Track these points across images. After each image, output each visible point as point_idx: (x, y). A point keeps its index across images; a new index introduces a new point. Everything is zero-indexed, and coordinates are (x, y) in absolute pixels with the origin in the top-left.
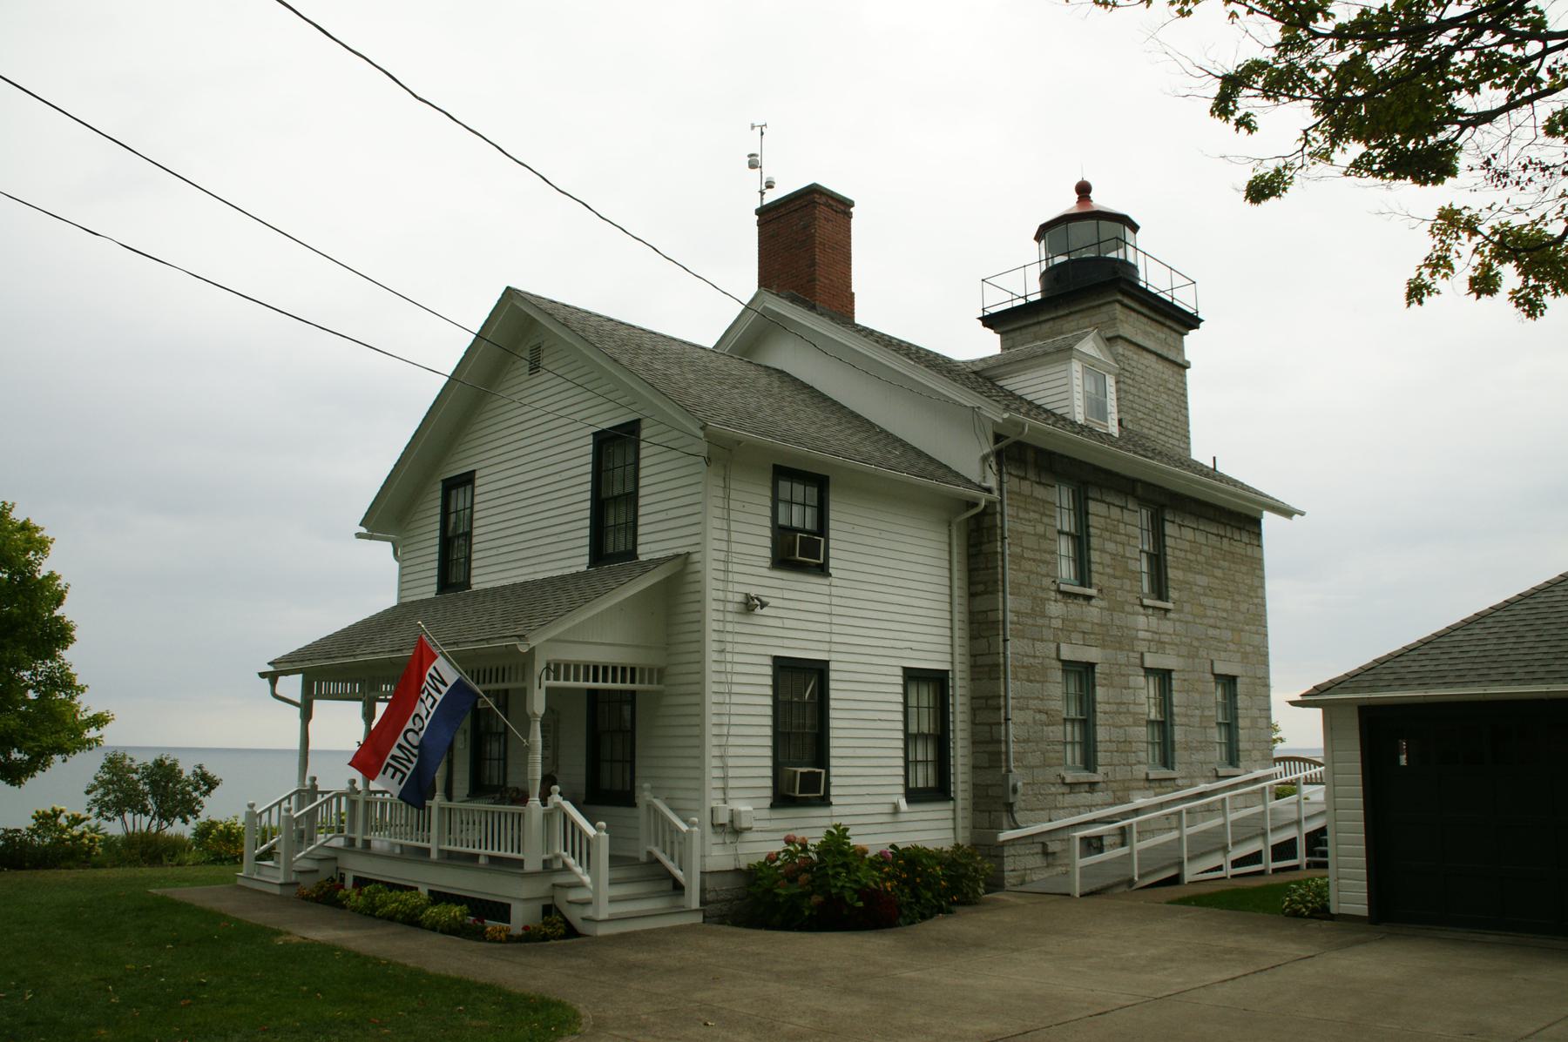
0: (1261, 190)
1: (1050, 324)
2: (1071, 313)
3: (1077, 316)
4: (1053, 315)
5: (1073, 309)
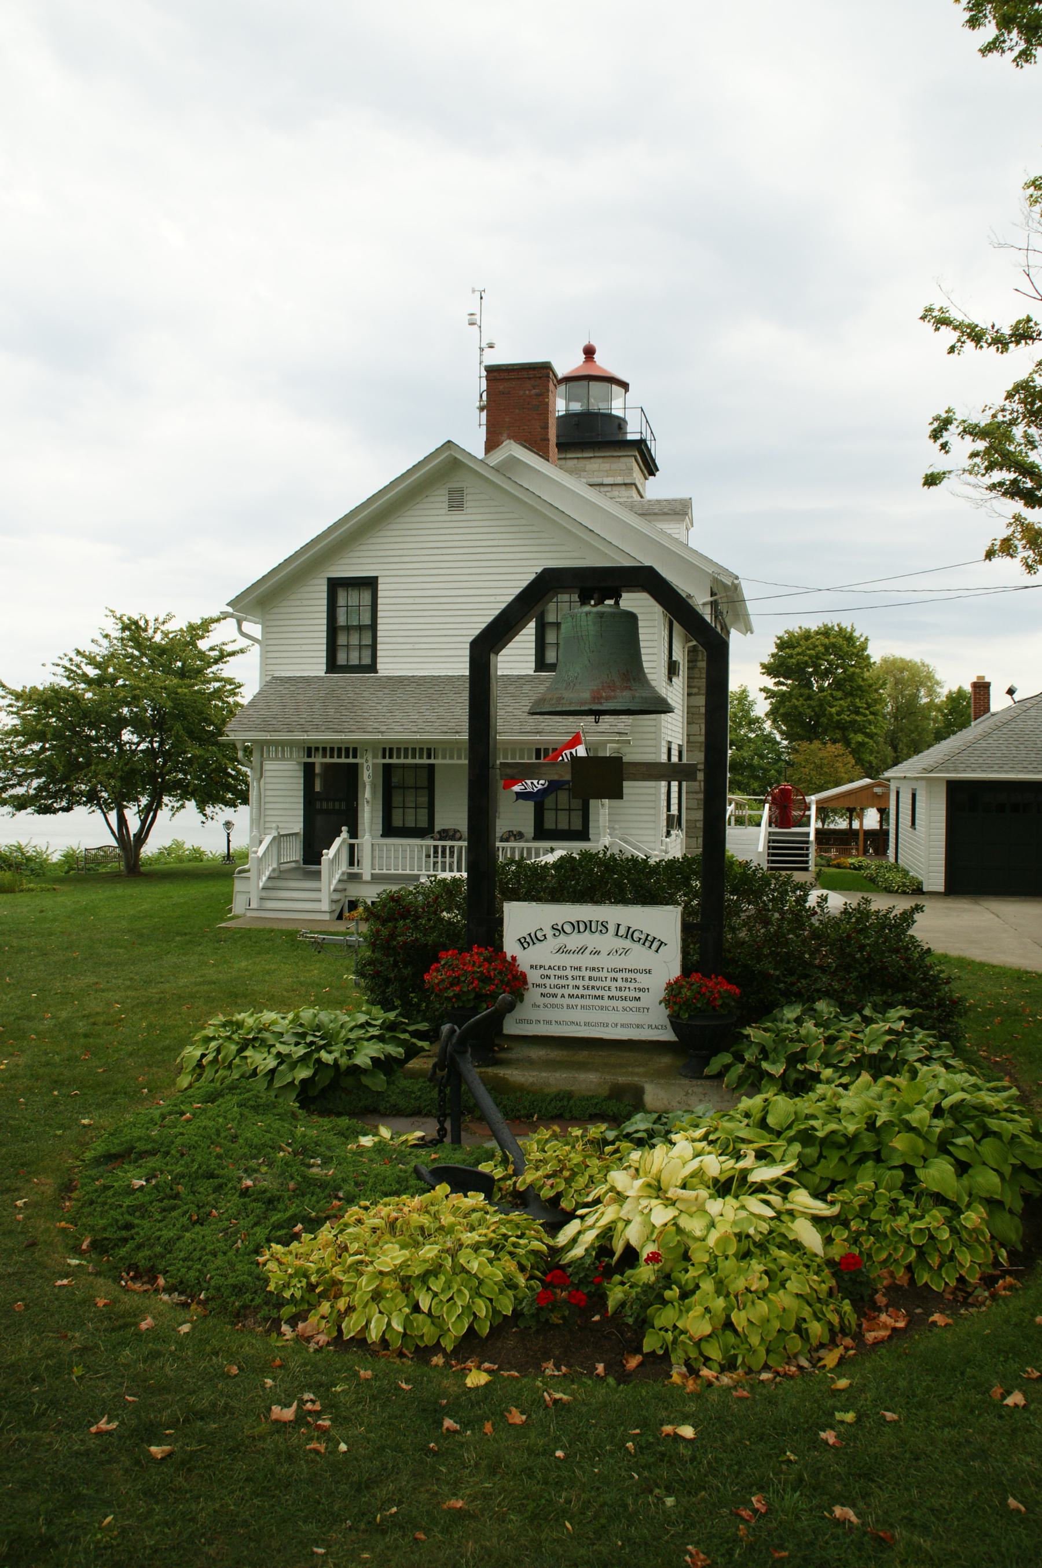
0: (932, 480)
1: (576, 461)
3: (600, 460)
5: (597, 454)
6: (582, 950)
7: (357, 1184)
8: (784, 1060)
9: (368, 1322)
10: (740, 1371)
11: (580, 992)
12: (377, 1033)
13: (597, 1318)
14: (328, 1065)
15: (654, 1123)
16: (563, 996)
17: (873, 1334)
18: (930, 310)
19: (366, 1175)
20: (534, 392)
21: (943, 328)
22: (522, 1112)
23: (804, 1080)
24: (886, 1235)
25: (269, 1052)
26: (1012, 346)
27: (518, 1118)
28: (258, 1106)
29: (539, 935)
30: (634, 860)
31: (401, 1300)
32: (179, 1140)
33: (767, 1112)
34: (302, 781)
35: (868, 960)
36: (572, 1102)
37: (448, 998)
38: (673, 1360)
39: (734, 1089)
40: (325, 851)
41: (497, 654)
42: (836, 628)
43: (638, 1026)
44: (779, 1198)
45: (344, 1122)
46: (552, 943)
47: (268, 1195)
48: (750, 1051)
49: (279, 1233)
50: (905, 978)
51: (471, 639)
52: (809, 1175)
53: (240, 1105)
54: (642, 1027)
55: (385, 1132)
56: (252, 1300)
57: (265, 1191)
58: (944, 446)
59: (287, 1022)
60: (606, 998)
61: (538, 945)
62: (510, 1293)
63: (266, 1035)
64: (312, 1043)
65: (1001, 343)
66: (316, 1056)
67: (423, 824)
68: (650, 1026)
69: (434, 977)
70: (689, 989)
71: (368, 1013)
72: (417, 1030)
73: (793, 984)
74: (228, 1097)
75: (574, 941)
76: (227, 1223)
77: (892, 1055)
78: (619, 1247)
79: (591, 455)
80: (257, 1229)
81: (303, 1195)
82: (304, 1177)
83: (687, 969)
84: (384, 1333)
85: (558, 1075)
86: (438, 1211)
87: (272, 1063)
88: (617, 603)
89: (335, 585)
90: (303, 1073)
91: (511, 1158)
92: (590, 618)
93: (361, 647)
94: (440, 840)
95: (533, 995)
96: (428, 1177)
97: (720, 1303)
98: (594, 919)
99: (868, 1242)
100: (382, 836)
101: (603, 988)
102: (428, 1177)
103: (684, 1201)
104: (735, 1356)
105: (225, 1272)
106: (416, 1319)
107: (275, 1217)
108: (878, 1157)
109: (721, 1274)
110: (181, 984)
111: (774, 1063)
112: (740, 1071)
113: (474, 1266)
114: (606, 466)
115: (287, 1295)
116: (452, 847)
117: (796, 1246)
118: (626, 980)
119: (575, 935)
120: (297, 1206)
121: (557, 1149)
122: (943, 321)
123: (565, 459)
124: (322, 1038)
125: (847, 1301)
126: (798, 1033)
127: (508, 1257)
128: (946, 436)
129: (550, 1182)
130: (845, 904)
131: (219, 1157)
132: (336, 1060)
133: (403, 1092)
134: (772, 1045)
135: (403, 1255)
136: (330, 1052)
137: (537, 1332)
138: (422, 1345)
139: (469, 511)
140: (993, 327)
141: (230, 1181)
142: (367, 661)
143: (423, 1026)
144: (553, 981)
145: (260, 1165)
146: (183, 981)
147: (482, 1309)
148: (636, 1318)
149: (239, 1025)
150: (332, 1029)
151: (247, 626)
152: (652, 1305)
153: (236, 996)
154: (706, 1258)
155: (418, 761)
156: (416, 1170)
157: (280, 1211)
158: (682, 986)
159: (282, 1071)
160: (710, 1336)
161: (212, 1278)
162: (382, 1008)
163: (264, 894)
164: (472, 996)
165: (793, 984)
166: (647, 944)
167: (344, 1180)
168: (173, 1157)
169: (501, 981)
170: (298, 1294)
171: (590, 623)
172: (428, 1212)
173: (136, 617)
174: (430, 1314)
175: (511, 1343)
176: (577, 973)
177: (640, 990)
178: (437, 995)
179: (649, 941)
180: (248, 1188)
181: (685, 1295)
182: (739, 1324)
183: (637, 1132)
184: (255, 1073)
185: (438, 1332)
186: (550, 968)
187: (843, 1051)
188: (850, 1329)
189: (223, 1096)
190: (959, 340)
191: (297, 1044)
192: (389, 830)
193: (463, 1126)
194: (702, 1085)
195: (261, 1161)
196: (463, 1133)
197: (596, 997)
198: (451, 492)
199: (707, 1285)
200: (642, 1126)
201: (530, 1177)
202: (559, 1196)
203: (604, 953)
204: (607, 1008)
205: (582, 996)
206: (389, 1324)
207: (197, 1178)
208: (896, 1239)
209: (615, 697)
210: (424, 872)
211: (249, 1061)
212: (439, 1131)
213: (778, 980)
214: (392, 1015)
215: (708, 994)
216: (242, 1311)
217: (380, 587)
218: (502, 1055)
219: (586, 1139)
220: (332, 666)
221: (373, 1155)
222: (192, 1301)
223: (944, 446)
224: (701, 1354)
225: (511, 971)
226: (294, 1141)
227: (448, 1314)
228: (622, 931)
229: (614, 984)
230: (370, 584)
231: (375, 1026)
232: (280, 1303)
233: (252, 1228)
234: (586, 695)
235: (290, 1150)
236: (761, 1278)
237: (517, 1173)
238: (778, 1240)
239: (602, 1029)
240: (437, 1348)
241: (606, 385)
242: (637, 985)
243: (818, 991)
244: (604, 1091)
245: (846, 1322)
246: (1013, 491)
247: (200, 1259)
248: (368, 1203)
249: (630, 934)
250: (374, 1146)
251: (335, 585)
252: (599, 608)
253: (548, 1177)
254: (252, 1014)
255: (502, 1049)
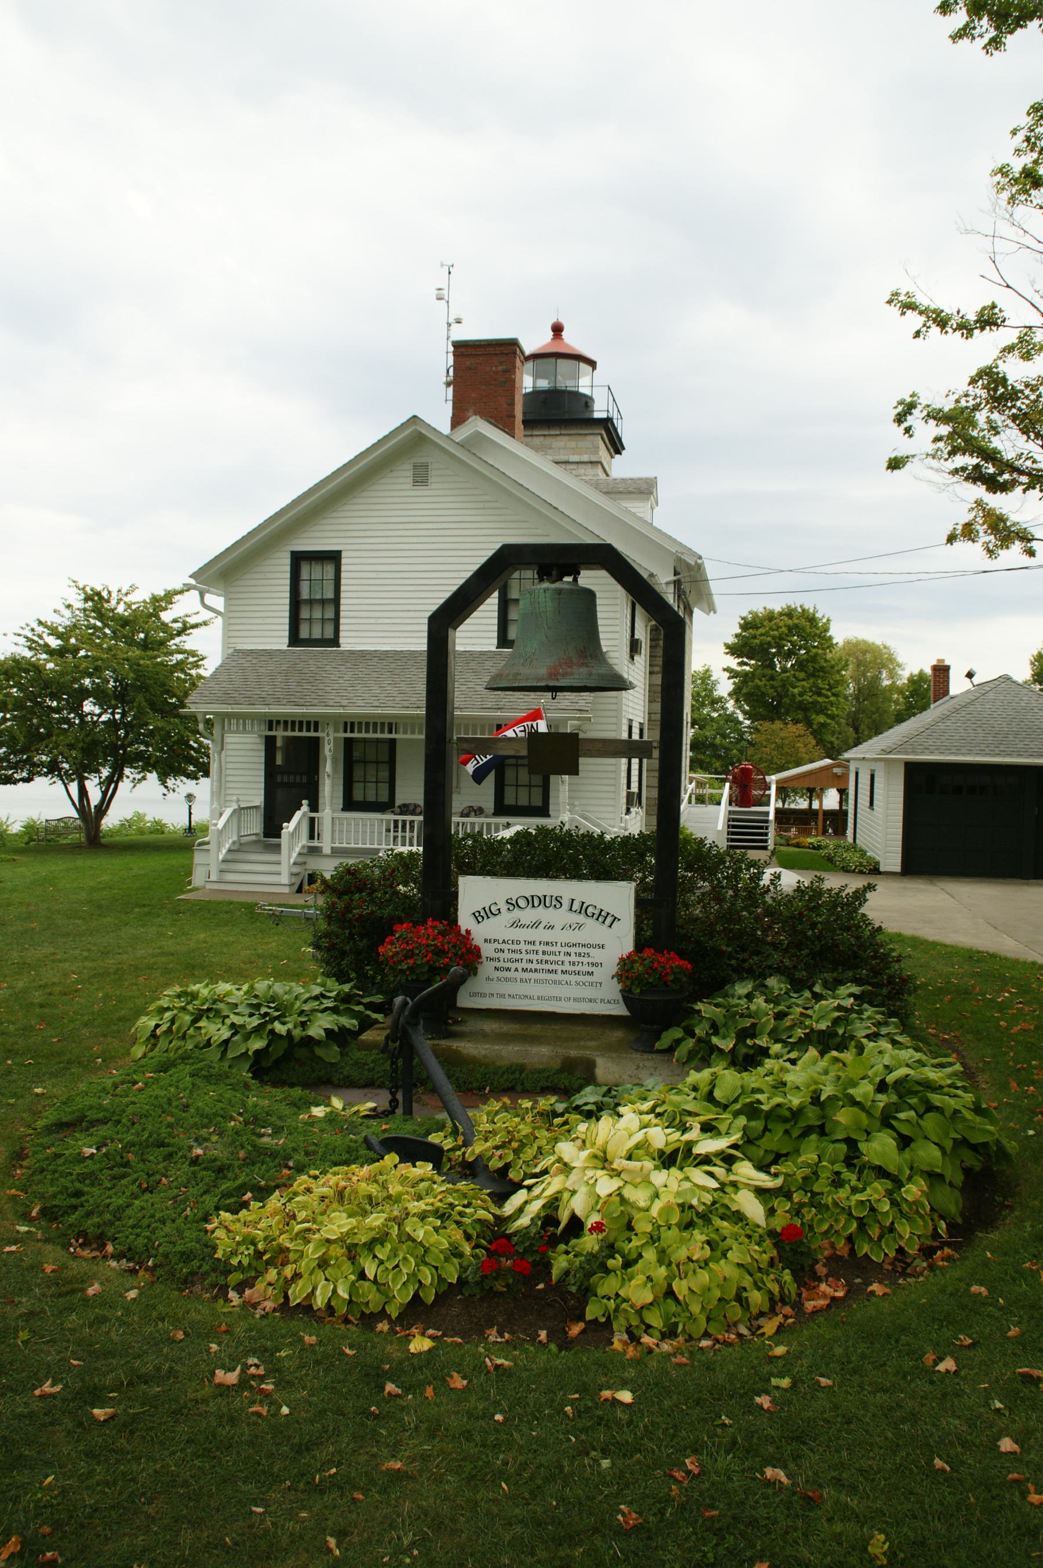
0: (895, 464)
1: (542, 438)
2: (561, 434)
3: (566, 438)
4: (546, 433)
5: (563, 432)
6: (536, 925)
7: (307, 1154)
8: (734, 1035)
9: (314, 1289)
10: (681, 1339)
11: (534, 966)
12: (331, 1005)
13: (541, 1286)
14: (281, 1036)
15: (604, 1096)
16: (516, 970)
17: (812, 1303)
18: (897, 294)
19: (316, 1145)
20: (500, 368)
21: (909, 312)
22: (475, 1085)
23: (753, 1055)
24: (827, 1207)
25: (223, 1023)
26: (977, 332)
27: (471, 1090)
28: (211, 1076)
29: (494, 909)
30: (589, 836)
31: (347, 1267)
32: (131, 1109)
33: (714, 1086)
34: (263, 754)
35: (819, 937)
36: (524, 1075)
37: (401, 970)
38: (615, 1327)
39: (684, 1063)
40: (285, 825)
41: (455, 628)
42: (799, 610)
43: (590, 1001)
44: (723, 1170)
45: (297, 1092)
46: (506, 917)
47: (218, 1163)
48: (701, 1026)
49: (228, 1201)
50: (856, 955)
51: (429, 614)
52: (754, 1148)
53: (192, 1075)
54: (595, 1001)
55: (337, 1103)
56: (200, 1267)
57: (215, 1160)
58: (907, 430)
59: (242, 993)
60: (559, 972)
61: (492, 919)
62: (456, 1261)
63: (221, 1006)
64: (266, 1014)
65: (966, 329)
66: (269, 1027)
67: (384, 798)
68: (602, 1001)
69: (389, 950)
70: (641, 964)
71: (323, 985)
72: (371, 1002)
73: (744, 960)
74: (181, 1067)
75: (528, 915)
76: (176, 1191)
77: (841, 1031)
78: (564, 1217)
79: (558, 432)
80: (206, 1197)
81: (253, 1164)
82: (254, 1146)
83: (640, 944)
84: (330, 1299)
85: (510, 1048)
86: (386, 1180)
87: (226, 1034)
88: (575, 580)
89: (298, 559)
90: (257, 1044)
91: (461, 1129)
92: (548, 594)
93: (323, 620)
94: (400, 814)
95: (486, 969)
96: (377, 1147)
97: (663, 1271)
98: (548, 894)
99: (810, 1213)
100: (343, 810)
101: (557, 963)
102: (377, 1147)
103: (629, 1171)
104: (676, 1324)
105: (173, 1239)
106: (362, 1286)
107: (225, 1186)
108: (822, 1131)
109: (663, 1244)
110: (139, 956)
111: (724, 1038)
112: (691, 1045)
113: (420, 1235)
114: (572, 444)
115: (234, 1261)
116: (412, 822)
117: (738, 1217)
118: (580, 954)
119: (529, 909)
120: (247, 1175)
121: (506, 1121)
122: (909, 306)
123: (532, 436)
124: (277, 1010)
125: (787, 1271)
126: (748, 1008)
127: (454, 1226)
128: (910, 420)
129: (499, 1152)
130: (799, 882)
131: (170, 1125)
132: (289, 1031)
133: (356, 1063)
134: (723, 1020)
135: (349, 1223)
136: (284, 1023)
137: (482, 1299)
138: (367, 1312)
139: (434, 486)
140: (958, 312)
141: (180, 1149)
142: (329, 634)
143: (378, 999)
144: (507, 955)
145: (211, 1134)
146: (140, 953)
147: (427, 1276)
148: (580, 1287)
149: (194, 996)
150: (287, 1000)
151: (209, 599)
152: (595, 1273)
153: (194, 967)
154: (649, 1228)
155: (379, 735)
156: (366, 1140)
157: (229, 1180)
158: (634, 961)
159: (235, 1042)
160: (651, 1304)
161: (160, 1245)
162: (337, 980)
163: (224, 866)
164: (426, 969)
165: (744, 960)
166: (601, 919)
167: (294, 1150)
168: (124, 1125)
169: (455, 954)
170: (246, 1262)
171: (548, 599)
172: (376, 1181)
173: (99, 588)
174: (375, 1281)
175: (455, 1310)
176: (530, 947)
177: (593, 964)
178: (391, 968)
179: (602, 916)
180: (198, 1157)
181: (628, 1264)
182: (680, 1292)
183: (586, 1104)
184: (208, 1044)
185: (383, 1299)
186: (504, 942)
187: (791, 1027)
188: (790, 1298)
189: (175, 1066)
190: (924, 325)
191: (251, 1015)
192: (350, 804)
193: (414, 1098)
194: (653, 1059)
195: (211, 1130)
196: (414, 1104)
197: (550, 971)
198: (415, 467)
199: (650, 1255)
200: (592, 1099)
201: (478, 1148)
202: (507, 1167)
203: (558, 927)
204: (560, 983)
205: (536, 970)
206: (334, 1291)
207: (147, 1147)
208: (838, 1211)
209: (571, 674)
210: (383, 846)
211: (203, 1031)
212: (390, 1102)
213: (730, 957)
214: (346, 988)
215: (660, 969)
216: (190, 1278)
217: (343, 561)
218: (455, 1028)
219: (535, 1111)
220: (295, 639)
221: (324, 1125)
222: (140, 1268)
223: (907, 430)
224: (643, 1321)
225: (465, 944)
226: (246, 1111)
227: (393, 1281)
228: (576, 906)
229: (567, 959)
230: (334, 557)
231: (330, 998)
232: (227, 1270)
233: (201, 1196)
234: (543, 671)
235: (241, 1119)
236: (703, 1248)
237: (466, 1144)
238: (721, 1211)
239: (552, 1003)
240: (383, 1314)
241: (575, 362)
242: (590, 960)
243: (769, 967)
244: (556, 1064)
245: (786, 1291)
246: (976, 476)
247: (149, 1226)
248: (317, 1173)
249: (583, 909)
250: (326, 1116)
251: (298, 559)
252: (558, 585)
253: (497, 1148)
254: (207, 985)
255: (456, 1022)
